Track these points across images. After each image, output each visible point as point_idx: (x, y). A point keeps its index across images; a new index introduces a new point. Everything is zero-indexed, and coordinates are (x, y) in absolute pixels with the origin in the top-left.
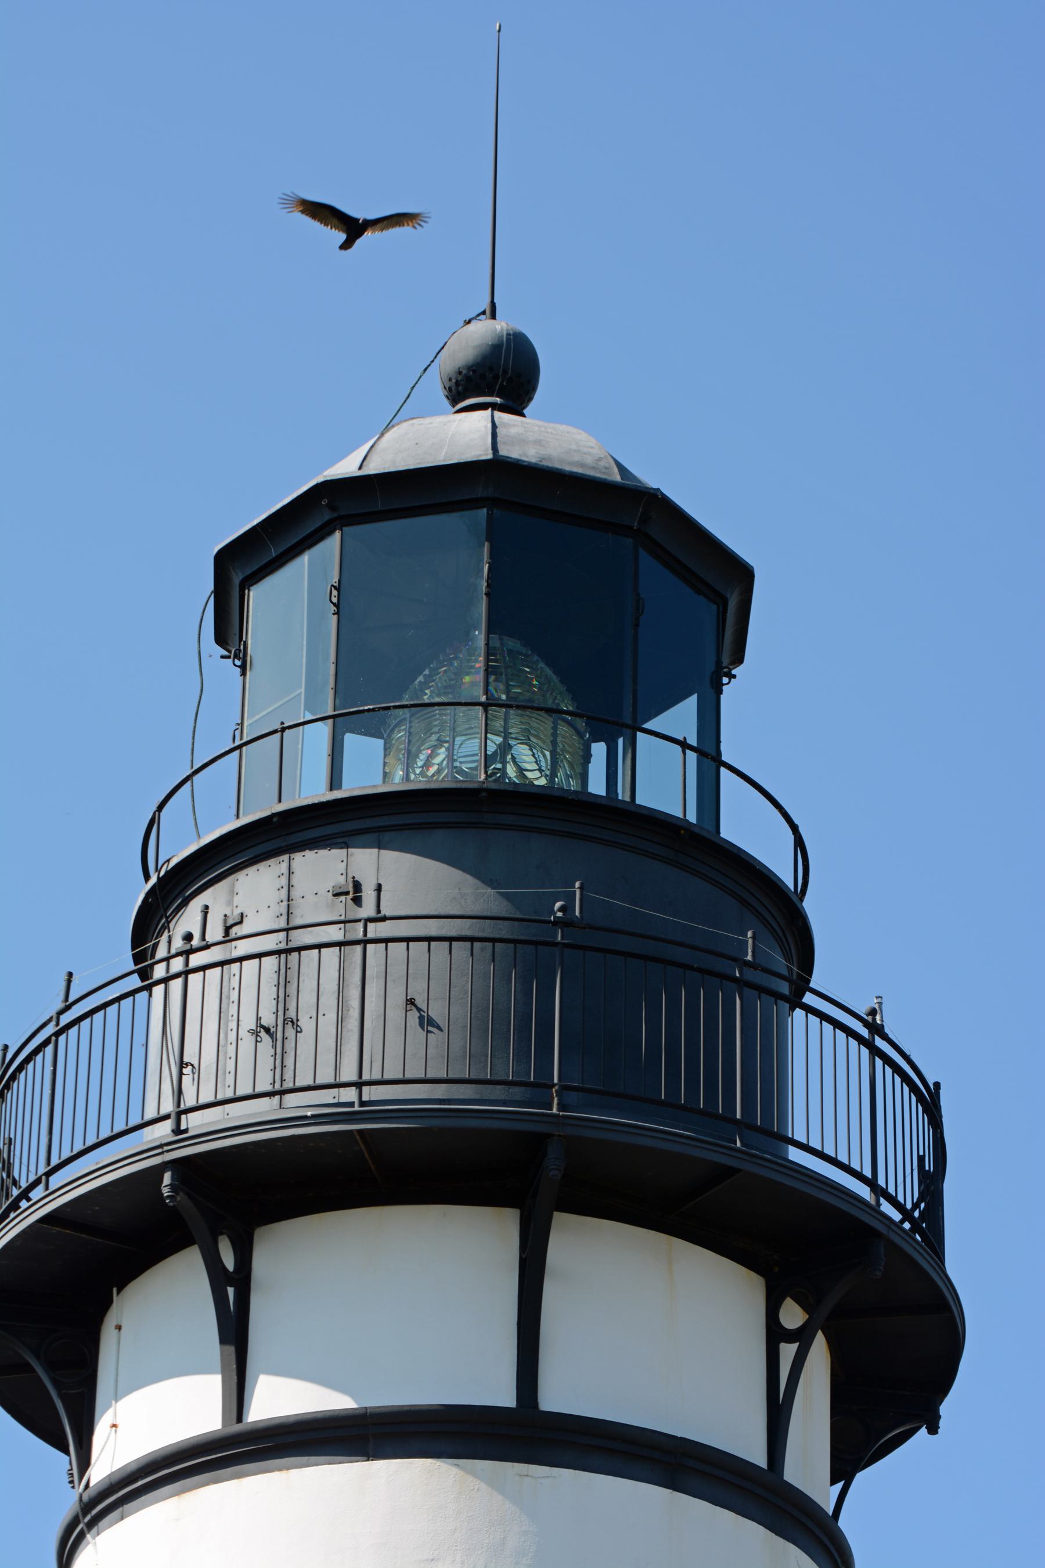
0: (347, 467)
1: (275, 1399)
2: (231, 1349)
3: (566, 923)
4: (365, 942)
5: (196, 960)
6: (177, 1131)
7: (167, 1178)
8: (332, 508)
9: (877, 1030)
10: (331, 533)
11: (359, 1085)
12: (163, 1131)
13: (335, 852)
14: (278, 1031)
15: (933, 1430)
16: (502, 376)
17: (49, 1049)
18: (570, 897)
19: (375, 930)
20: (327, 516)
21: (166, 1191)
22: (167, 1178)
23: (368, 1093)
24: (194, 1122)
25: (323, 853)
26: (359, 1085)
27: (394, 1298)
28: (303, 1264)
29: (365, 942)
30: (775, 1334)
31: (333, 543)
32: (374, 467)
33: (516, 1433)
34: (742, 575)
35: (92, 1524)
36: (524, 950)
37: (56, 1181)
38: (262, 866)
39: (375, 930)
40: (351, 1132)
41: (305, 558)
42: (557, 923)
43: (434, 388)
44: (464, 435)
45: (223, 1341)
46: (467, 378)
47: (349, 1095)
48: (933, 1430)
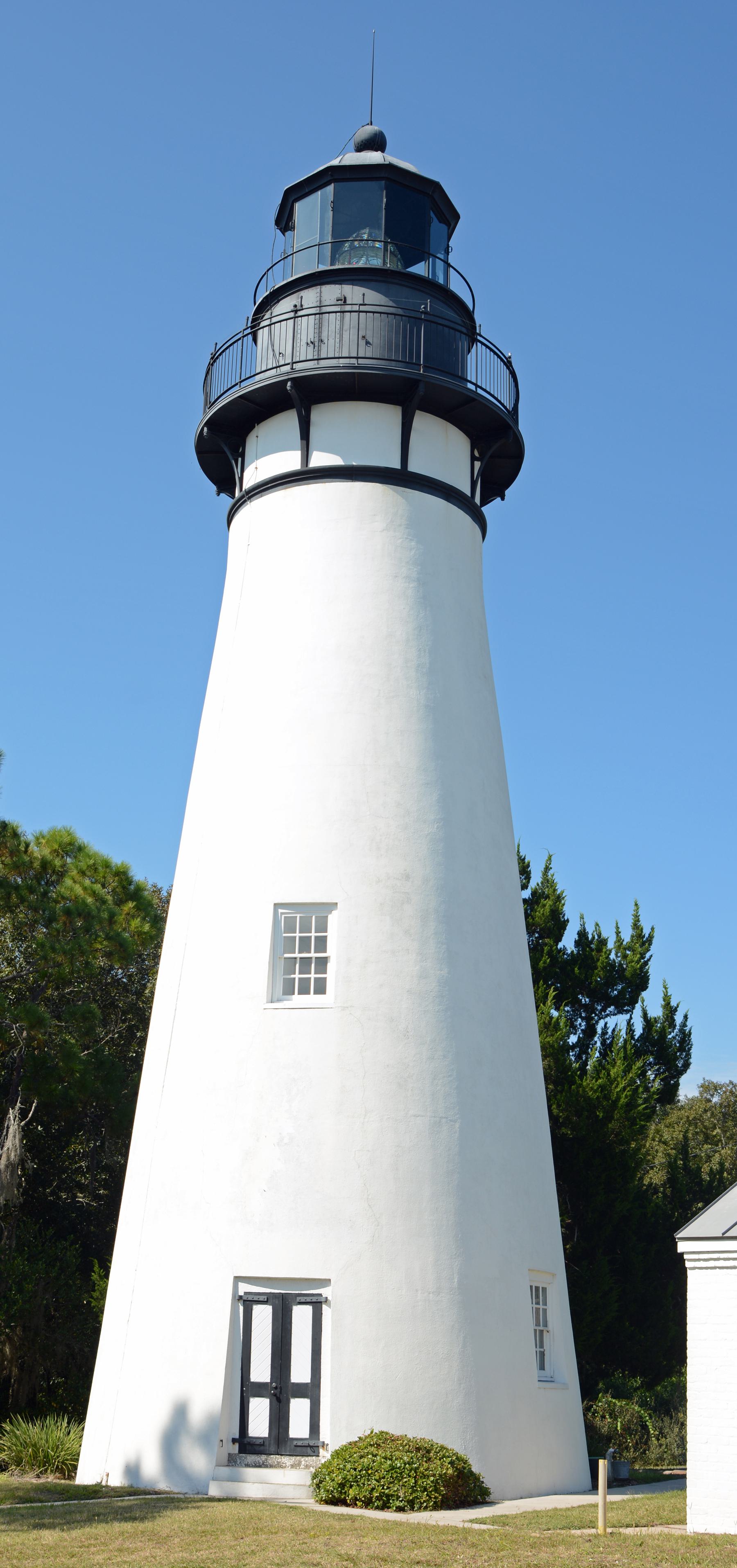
0: (335, 162)
1: (320, 459)
2: (305, 442)
3: (425, 313)
4: (360, 312)
5: (300, 313)
6: (292, 369)
7: (289, 384)
8: (332, 176)
9: (510, 363)
10: (327, 184)
11: (357, 358)
12: (287, 368)
13: (337, 286)
14: (317, 343)
15: (503, 499)
16: (376, 143)
17: (240, 342)
18: (426, 304)
19: (363, 308)
20: (329, 178)
21: (288, 388)
22: (289, 384)
23: (360, 361)
24: (298, 366)
25: (333, 286)
26: (357, 358)
27: (361, 430)
28: (327, 417)
29: (360, 312)
30: (473, 459)
31: (330, 188)
32: (344, 163)
33: (400, 477)
34: (457, 217)
35: (249, 498)
36: (409, 319)
37: (243, 384)
38: (310, 290)
39: (363, 308)
40: (354, 373)
41: (319, 192)
42: (422, 312)
43: (352, 145)
44: (373, 157)
45: (302, 439)
46: (365, 144)
47: (354, 361)
48: (503, 499)
